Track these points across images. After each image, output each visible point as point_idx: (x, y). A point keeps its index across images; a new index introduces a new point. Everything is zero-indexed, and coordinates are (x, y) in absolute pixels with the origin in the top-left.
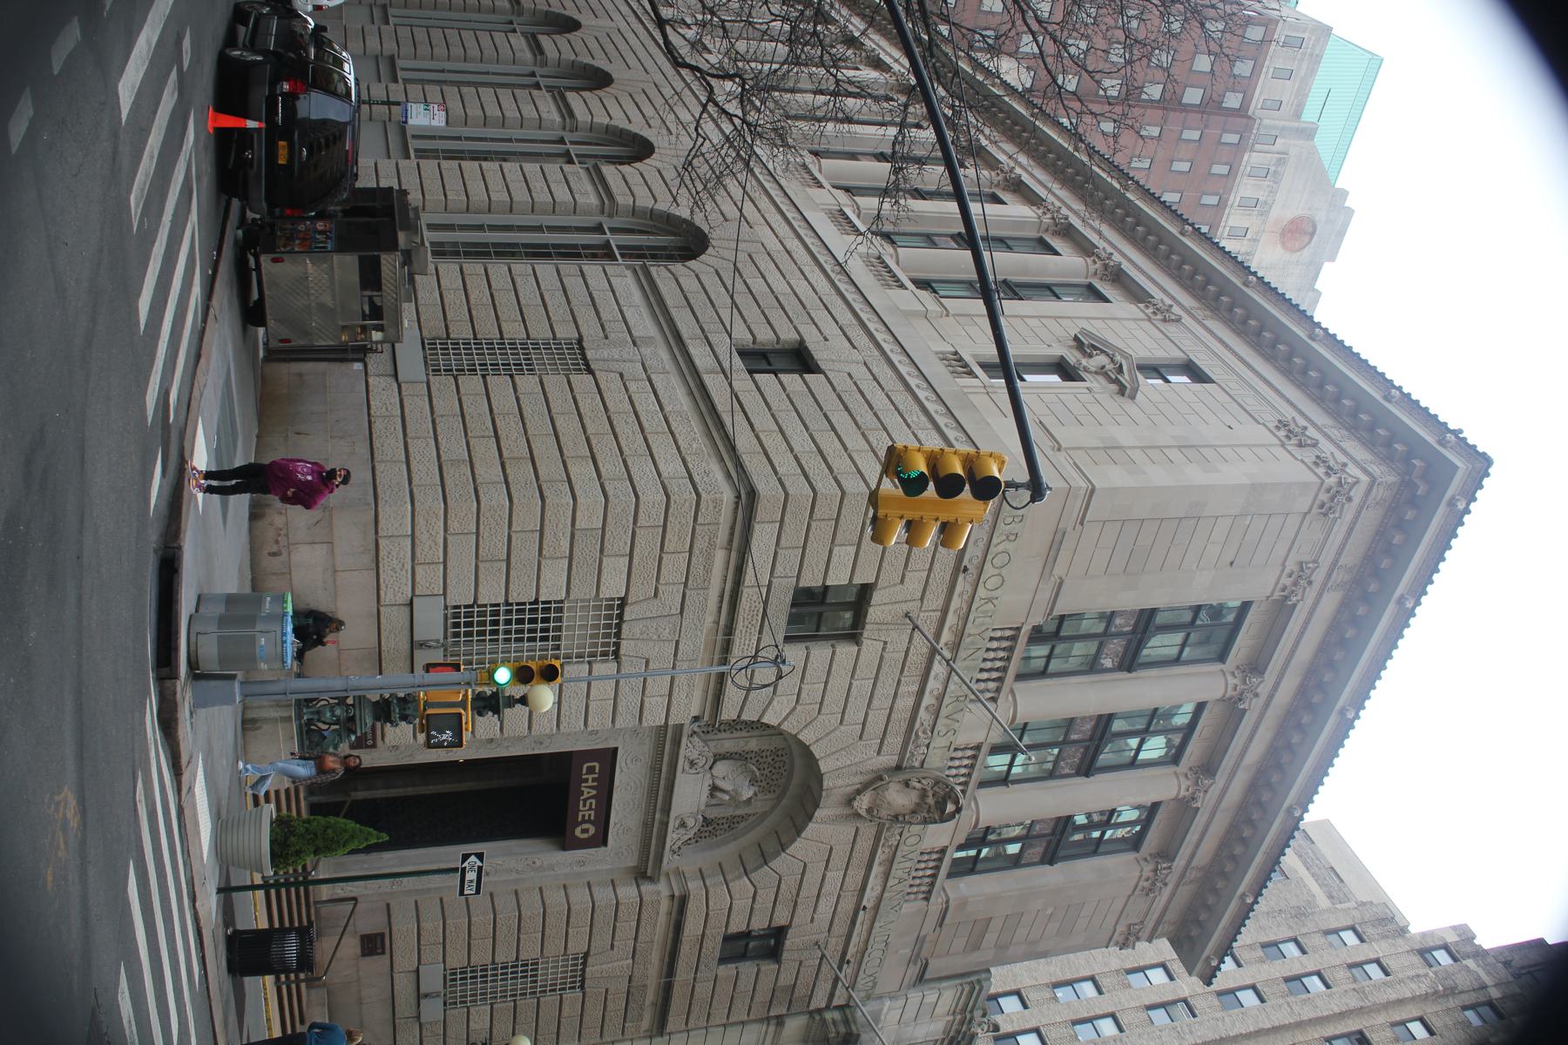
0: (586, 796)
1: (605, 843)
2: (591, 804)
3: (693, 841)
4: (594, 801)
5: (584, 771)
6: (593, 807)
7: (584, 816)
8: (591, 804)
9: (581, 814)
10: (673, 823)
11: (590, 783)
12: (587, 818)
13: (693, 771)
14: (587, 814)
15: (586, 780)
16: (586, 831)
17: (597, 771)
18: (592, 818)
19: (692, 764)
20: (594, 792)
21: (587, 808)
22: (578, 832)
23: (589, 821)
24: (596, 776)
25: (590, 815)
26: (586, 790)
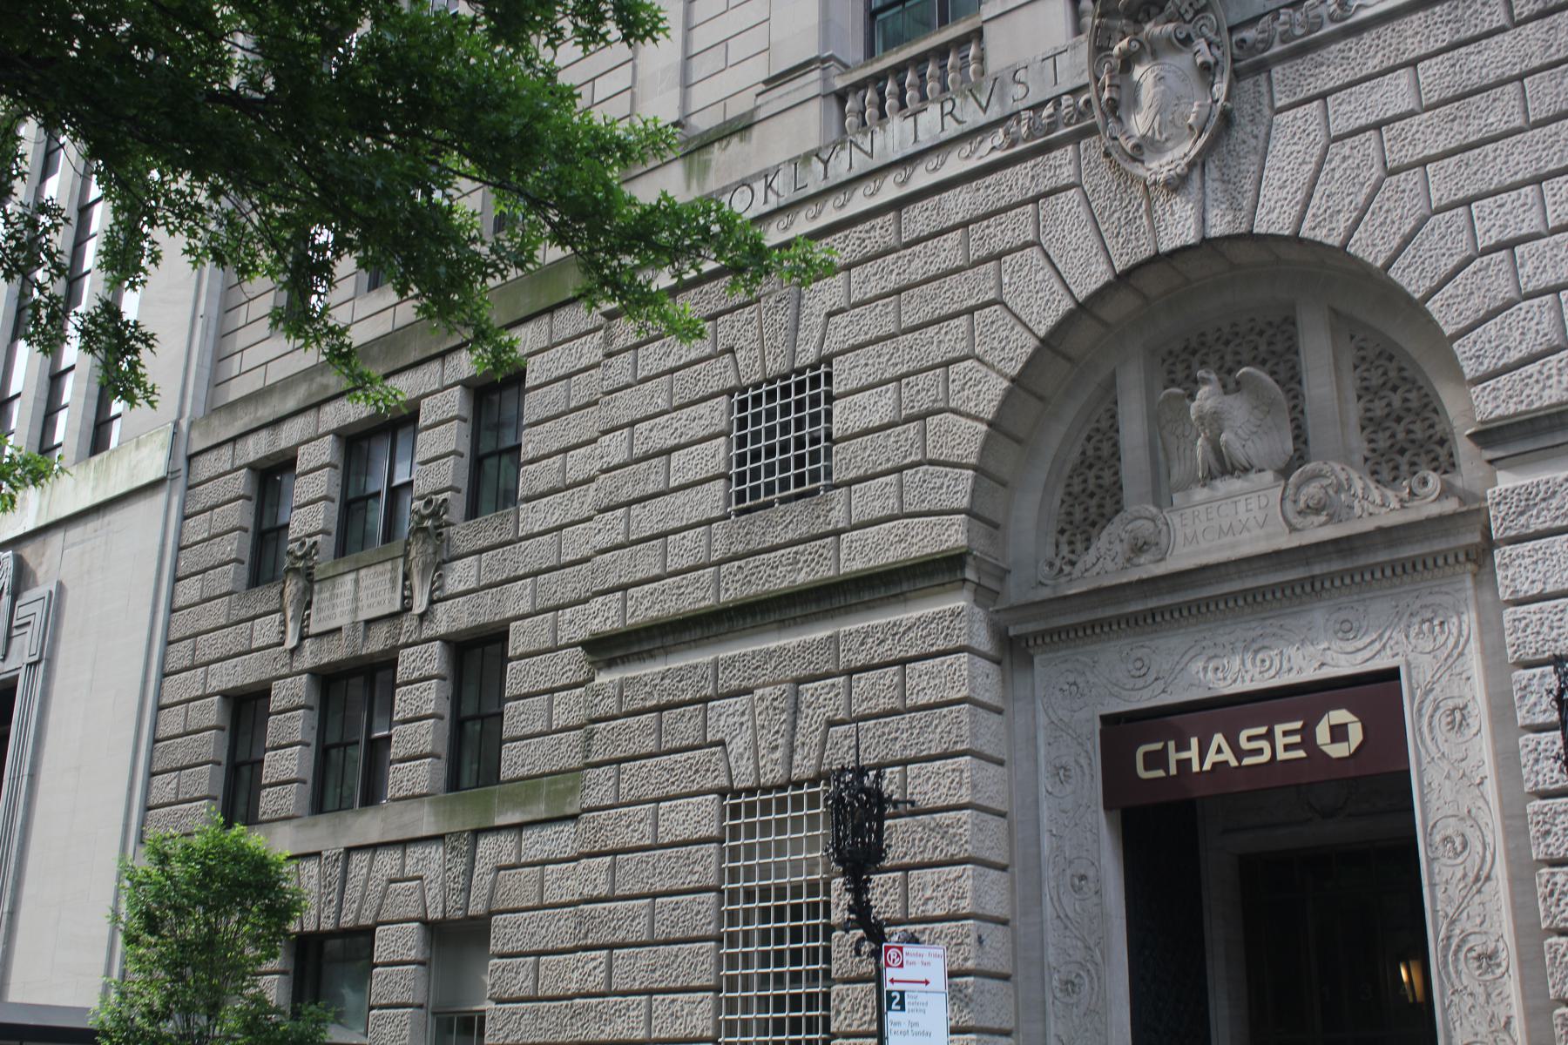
0: (1228, 756)
1: (1392, 675)
2: (1250, 739)
3: (1442, 452)
4: (1244, 735)
5: (1160, 773)
6: (1263, 730)
7: (1287, 748)
8: (1250, 739)
9: (1282, 755)
10: (1318, 531)
11: (1193, 754)
12: (1297, 739)
13: (1163, 540)
14: (1280, 741)
15: (1184, 764)
16: (1339, 733)
17: (1158, 746)
18: (1298, 725)
19: (1139, 548)
20: (1218, 739)
21: (1264, 744)
22: (1339, 751)
23: (1308, 734)
24: (1172, 745)
25: (1286, 734)
26: (1212, 757)
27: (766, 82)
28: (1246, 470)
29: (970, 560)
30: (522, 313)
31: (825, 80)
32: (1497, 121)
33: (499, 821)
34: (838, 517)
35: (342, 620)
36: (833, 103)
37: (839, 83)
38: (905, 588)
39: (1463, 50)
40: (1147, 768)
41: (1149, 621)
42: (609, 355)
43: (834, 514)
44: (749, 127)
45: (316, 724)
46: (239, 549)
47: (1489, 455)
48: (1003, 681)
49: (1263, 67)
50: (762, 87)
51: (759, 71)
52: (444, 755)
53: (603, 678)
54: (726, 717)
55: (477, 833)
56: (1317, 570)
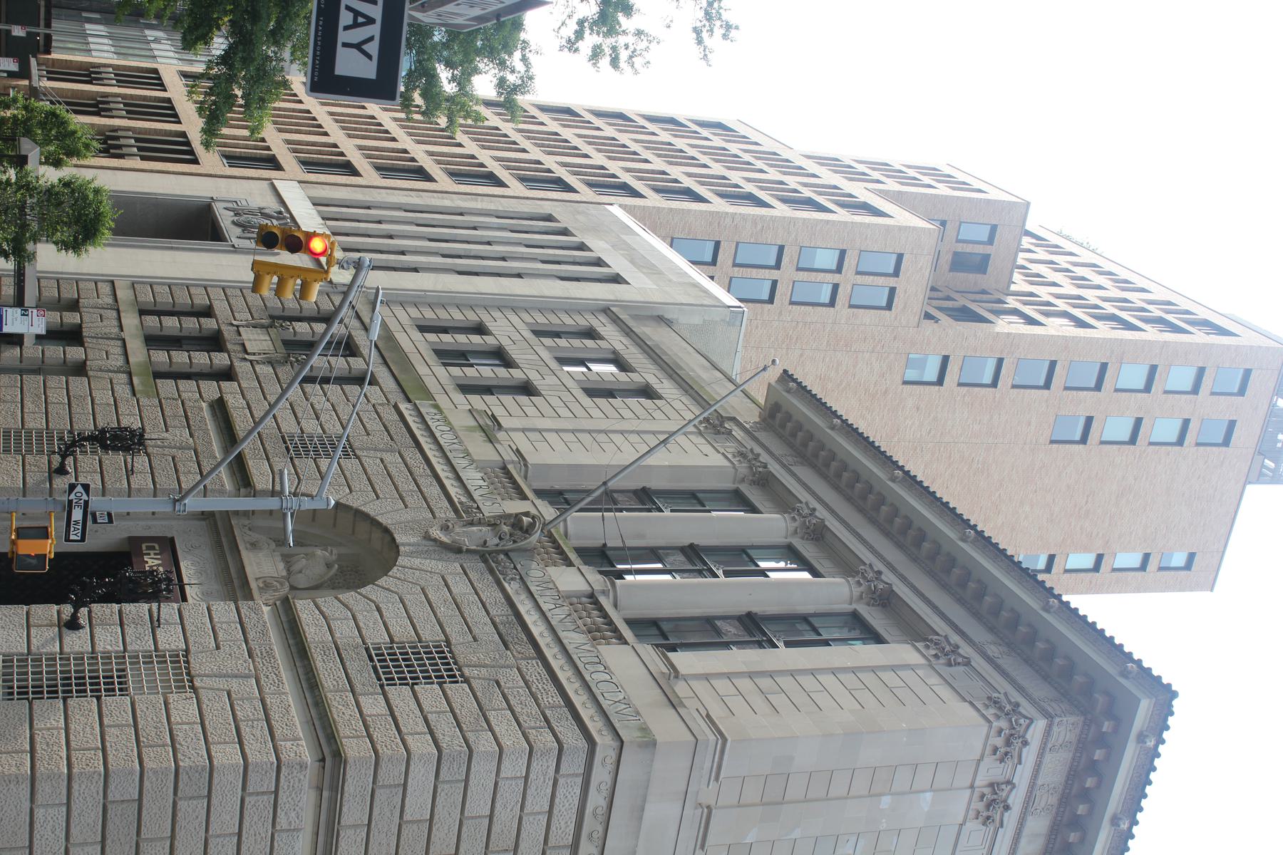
11: (152, 556)
20: (160, 562)
27: (518, 450)
28: (289, 570)
29: (249, 489)
30: (403, 384)
31: (513, 462)
32: (441, 611)
33: (135, 380)
34: (274, 460)
35: (244, 336)
36: (502, 465)
37: (510, 467)
38: (238, 475)
39: (480, 605)
40: (147, 546)
41: (218, 544)
42: (374, 406)
43: (278, 459)
44: (491, 442)
45: (192, 335)
46: (290, 309)
47: (278, 603)
48: (194, 515)
49: (485, 561)
50: (514, 448)
51: (525, 448)
52: (172, 369)
53: (204, 405)
54: (180, 434)
55: (130, 375)
56: (236, 581)
